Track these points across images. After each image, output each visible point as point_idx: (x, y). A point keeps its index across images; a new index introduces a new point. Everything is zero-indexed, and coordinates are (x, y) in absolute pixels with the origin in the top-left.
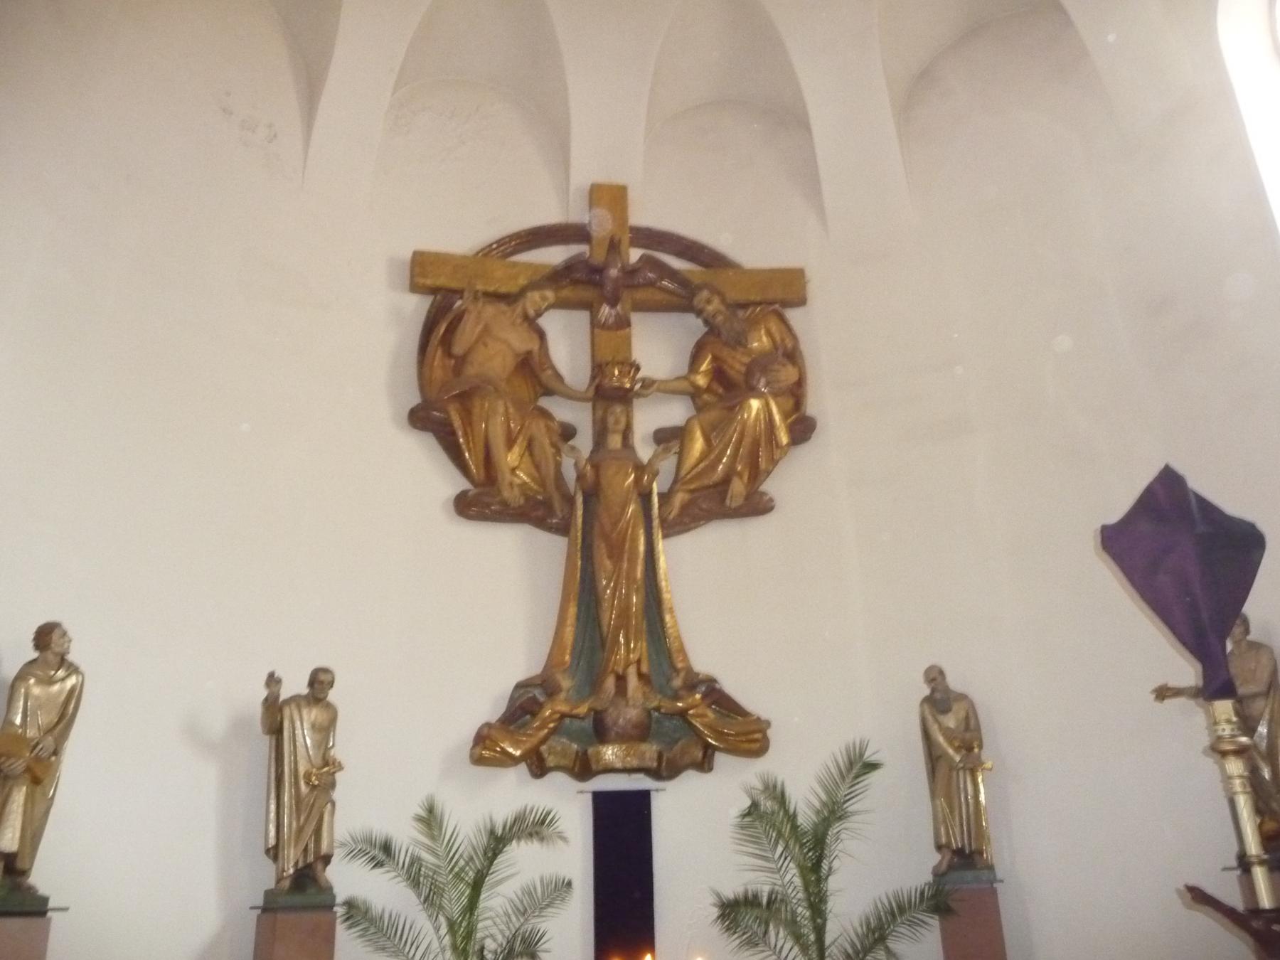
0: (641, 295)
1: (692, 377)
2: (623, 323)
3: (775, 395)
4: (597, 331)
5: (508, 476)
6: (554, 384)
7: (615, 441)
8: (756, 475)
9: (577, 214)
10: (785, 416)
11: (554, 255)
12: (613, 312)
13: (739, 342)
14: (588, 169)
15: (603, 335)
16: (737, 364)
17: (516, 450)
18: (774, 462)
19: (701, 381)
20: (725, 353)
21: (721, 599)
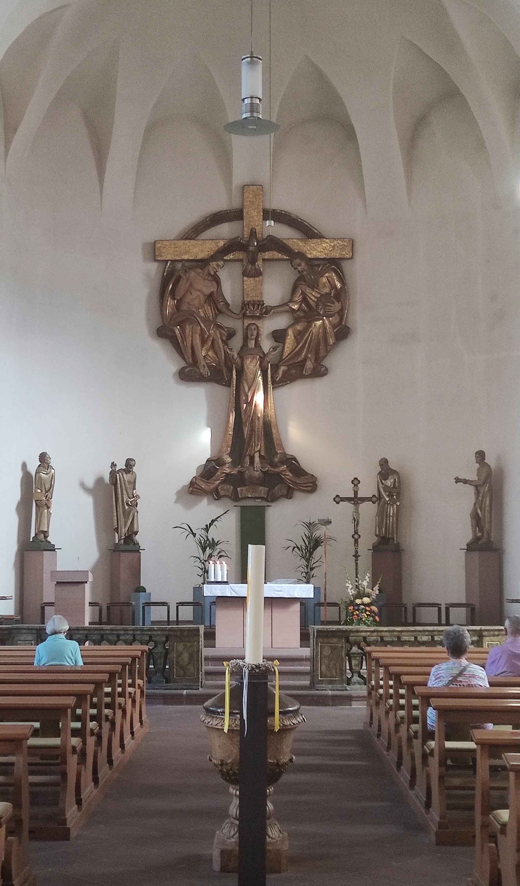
0: (267, 255)
1: (291, 305)
2: (258, 274)
3: (328, 317)
4: (245, 278)
5: (203, 363)
6: (224, 310)
7: (252, 344)
8: (318, 359)
9: (236, 204)
10: (334, 326)
11: (226, 231)
12: (253, 268)
13: (314, 286)
14: (240, 175)
15: (249, 282)
16: (313, 296)
17: (206, 347)
18: (327, 352)
19: (295, 307)
20: (308, 291)
21: (301, 422)
